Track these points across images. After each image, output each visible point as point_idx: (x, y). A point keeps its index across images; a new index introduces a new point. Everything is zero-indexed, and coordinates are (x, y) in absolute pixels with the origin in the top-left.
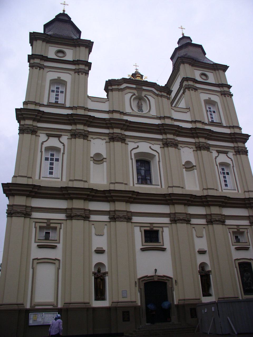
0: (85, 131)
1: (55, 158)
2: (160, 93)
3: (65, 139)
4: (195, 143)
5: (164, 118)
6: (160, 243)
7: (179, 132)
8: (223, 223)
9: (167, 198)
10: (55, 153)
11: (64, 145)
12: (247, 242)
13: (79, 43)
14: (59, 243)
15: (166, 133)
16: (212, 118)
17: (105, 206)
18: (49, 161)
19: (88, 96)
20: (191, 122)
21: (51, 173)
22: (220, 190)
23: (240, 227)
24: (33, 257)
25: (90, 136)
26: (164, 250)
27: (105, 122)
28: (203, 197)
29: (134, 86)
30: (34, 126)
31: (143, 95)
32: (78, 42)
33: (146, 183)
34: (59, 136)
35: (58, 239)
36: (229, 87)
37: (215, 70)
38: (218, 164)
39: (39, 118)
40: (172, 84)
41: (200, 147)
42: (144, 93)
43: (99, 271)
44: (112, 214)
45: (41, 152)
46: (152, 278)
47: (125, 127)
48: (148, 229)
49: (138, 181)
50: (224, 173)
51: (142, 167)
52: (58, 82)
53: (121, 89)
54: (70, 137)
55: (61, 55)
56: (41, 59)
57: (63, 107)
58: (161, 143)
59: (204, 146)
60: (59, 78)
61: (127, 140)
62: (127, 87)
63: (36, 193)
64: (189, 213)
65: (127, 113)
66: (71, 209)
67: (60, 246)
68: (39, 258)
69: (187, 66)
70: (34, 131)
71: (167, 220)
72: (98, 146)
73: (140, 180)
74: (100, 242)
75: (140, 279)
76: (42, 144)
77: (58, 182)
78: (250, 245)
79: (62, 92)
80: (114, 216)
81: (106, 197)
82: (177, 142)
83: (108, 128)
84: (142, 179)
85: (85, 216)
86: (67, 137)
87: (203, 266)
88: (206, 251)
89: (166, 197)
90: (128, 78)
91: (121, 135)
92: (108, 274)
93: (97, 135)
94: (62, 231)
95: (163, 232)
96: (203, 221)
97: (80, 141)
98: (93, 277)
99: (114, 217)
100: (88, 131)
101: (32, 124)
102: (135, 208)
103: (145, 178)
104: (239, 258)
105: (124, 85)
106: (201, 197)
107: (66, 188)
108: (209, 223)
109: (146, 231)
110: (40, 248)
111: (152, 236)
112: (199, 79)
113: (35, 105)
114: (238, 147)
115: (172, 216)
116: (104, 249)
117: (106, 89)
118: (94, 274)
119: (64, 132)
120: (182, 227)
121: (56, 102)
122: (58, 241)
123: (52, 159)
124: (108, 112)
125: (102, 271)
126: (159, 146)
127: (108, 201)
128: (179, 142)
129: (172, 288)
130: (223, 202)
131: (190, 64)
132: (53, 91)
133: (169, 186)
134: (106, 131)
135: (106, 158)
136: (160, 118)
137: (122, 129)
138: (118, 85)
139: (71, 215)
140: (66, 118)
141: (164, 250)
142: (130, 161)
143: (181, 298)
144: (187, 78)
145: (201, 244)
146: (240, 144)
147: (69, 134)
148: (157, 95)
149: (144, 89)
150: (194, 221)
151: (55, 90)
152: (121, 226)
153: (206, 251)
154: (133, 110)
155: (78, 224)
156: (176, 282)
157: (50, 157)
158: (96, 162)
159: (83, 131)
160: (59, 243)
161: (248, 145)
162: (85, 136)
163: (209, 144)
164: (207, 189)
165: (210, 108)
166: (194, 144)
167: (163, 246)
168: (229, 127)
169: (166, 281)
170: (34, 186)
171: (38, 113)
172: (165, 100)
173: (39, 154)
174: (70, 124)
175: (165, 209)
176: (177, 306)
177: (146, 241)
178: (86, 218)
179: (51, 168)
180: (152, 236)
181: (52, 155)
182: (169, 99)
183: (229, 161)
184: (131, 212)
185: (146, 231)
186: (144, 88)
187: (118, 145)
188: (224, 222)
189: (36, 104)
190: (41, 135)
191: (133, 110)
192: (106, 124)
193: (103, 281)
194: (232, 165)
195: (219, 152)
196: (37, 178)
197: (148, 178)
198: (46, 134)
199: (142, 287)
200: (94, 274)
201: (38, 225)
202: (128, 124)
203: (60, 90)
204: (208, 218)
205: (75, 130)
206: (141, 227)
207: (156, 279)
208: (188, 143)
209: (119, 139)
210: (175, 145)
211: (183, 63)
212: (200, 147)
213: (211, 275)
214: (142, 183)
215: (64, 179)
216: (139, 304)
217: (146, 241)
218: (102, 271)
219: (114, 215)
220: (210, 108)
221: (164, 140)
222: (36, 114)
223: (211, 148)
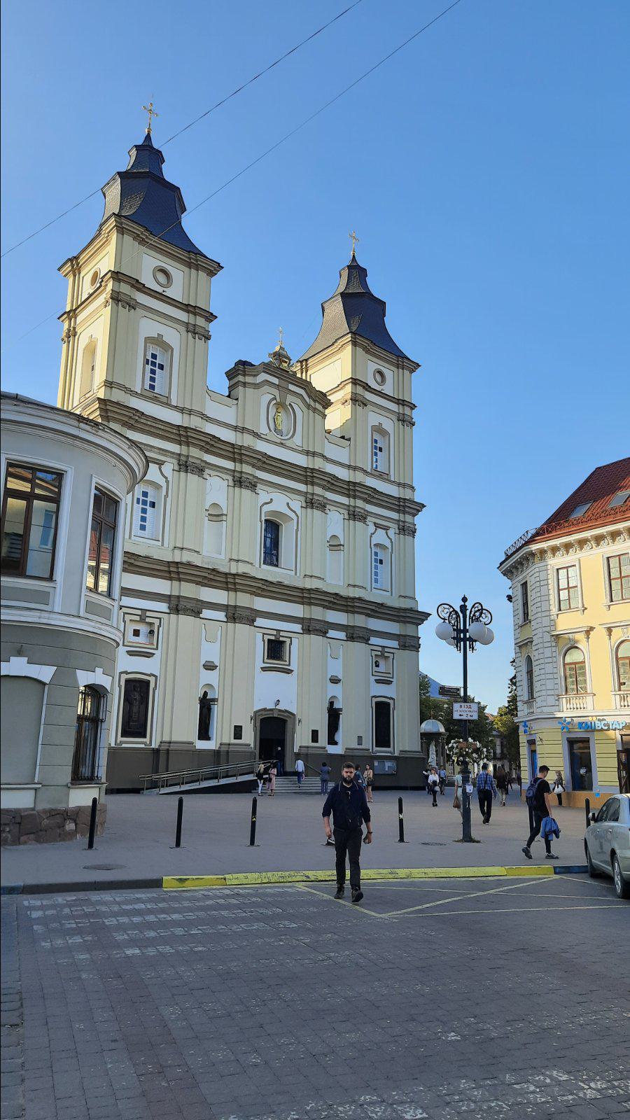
0: (202, 461)
1: (149, 499)
2: (312, 403)
3: (169, 468)
4: (349, 506)
5: (314, 454)
6: (286, 661)
7: (333, 484)
8: (366, 641)
10: (150, 490)
11: (167, 482)
12: (390, 673)
14: (157, 649)
15: (313, 484)
17: (220, 596)
19: (208, 391)
20: (349, 467)
21: (143, 528)
22: (369, 588)
23: (386, 650)
24: (119, 668)
26: (289, 672)
27: (231, 449)
28: (349, 600)
29: (276, 381)
31: (287, 403)
32: (197, 260)
33: (272, 564)
35: (155, 643)
36: (413, 407)
38: (372, 546)
39: (132, 422)
41: (354, 516)
42: (290, 399)
46: (271, 712)
48: (273, 638)
53: (258, 384)
54: (177, 468)
56: (133, 286)
58: (303, 499)
62: (266, 381)
65: (262, 436)
71: (297, 628)
72: (216, 489)
74: (211, 652)
75: (256, 713)
78: (393, 678)
80: (234, 614)
81: (227, 583)
82: (325, 501)
83: (234, 460)
85: (195, 609)
90: (267, 360)
92: (217, 701)
95: (291, 644)
99: (235, 615)
100: (205, 462)
102: (261, 604)
103: (272, 554)
104: (377, 695)
105: (263, 377)
106: (347, 599)
108: (349, 639)
110: (130, 655)
114: (404, 522)
117: (231, 375)
120: (315, 639)
121: (152, 387)
122: (155, 647)
123: (145, 503)
127: (228, 589)
130: (372, 610)
134: (229, 465)
136: (308, 453)
137: (253, 466)
139: (178, 606)
140: (174, 431)
145: (336, 668)
146: (408, 518)
148: (308, 406)
149: (290, 390)
150: (332, 633)
151: (150, 359)
152: (241, 628)
155: (186, 621)
156: (299, 721)
157: (141, 498)
158: (211, 518)
159: (198, 462)
160: (157, 649)
161: (420, 520)
162: (200, 470)
163: (368, 511)
164: (354, 586)
167: (289, 665)
168: (399, 484)
177: (269, 657)
178: (196, 613)
180: (275, 649)
183: (387, 543)
186: (291, 387)
187: (246, 493)
188: (369, 639)
192: (234, 453)
193: (209, 710)
194: (390, 551)
199: (258, 724)
201: (128, 617)
202: (265, 460)
203: (158, 362)
205: (188, 456)
208: (338, 505)
217: (269, 657)
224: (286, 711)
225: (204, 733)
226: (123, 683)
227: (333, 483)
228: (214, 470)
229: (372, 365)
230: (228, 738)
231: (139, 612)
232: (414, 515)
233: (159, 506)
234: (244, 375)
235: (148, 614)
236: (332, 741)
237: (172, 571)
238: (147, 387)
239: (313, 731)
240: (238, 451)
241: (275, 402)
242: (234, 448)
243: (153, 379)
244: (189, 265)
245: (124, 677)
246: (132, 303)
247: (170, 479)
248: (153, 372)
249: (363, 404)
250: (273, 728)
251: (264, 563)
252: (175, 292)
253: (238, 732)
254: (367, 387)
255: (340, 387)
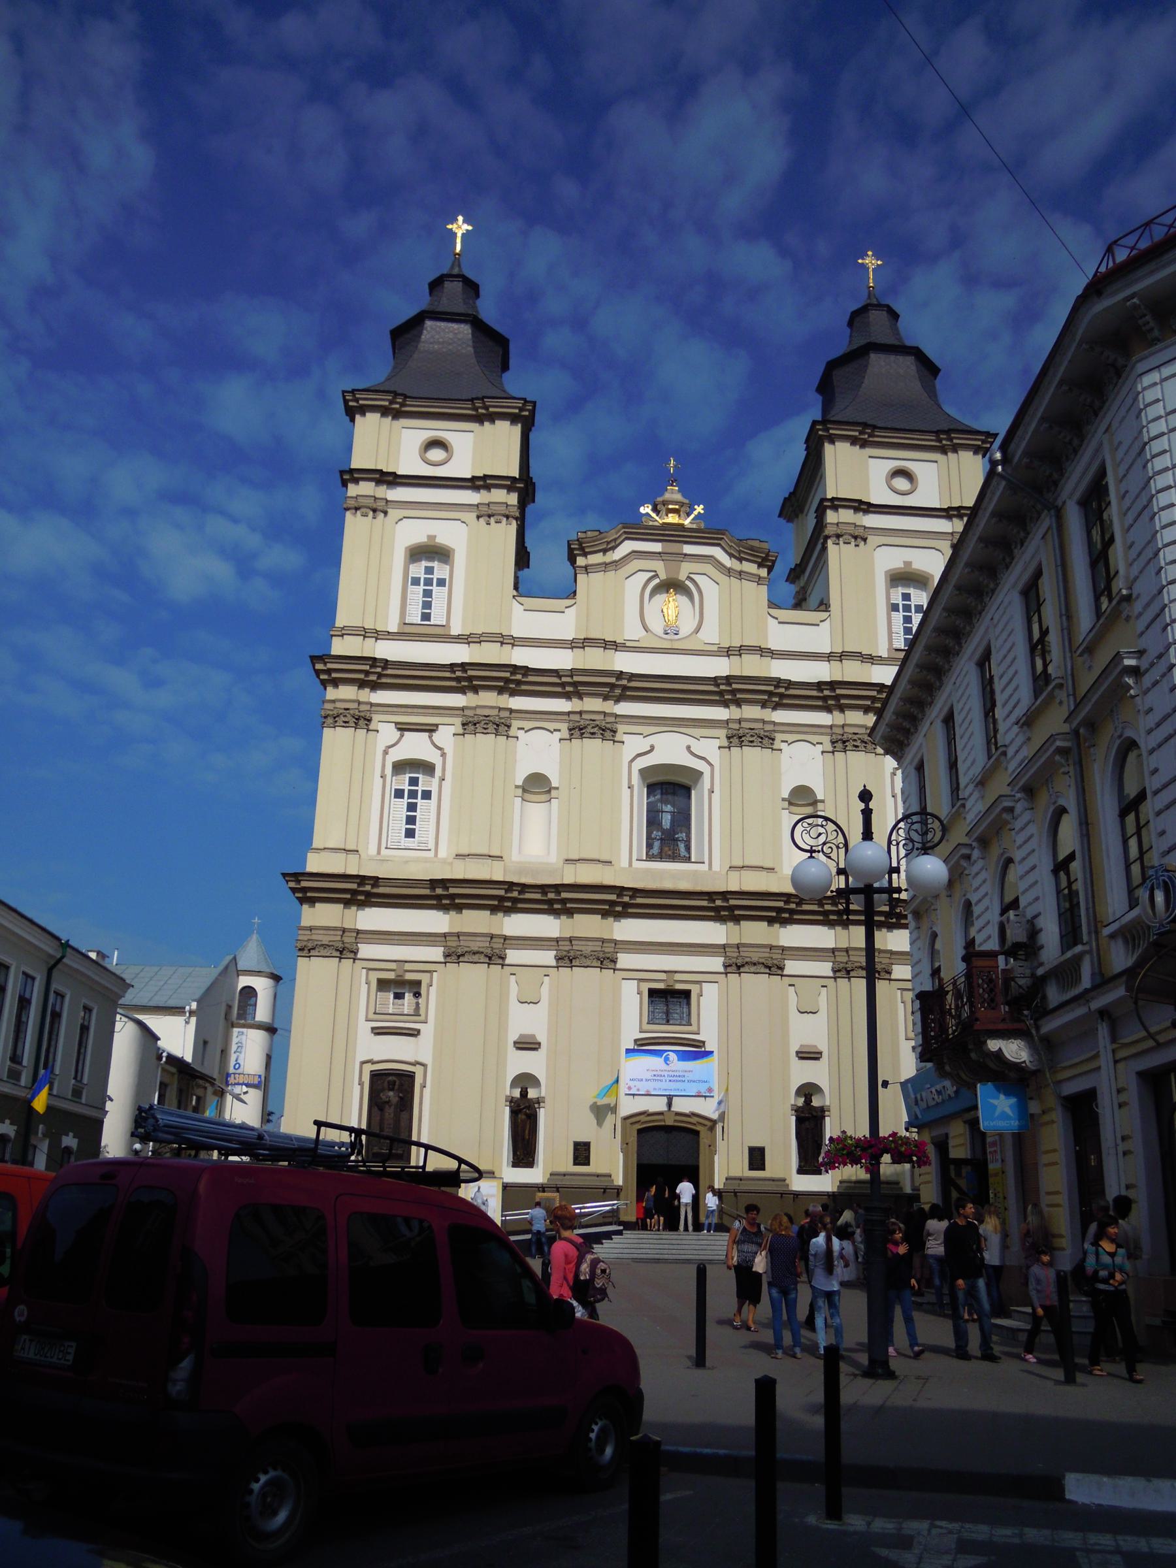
0: (500, 709)
1: (420, 788)
3: (446, 735)
4: (831, 727)
5: (741, 651)
9: (719, 903)
11: (443, 755)
13: (491, 410)
15: (738, 703)
18: (405, 800)
20: (829, 657)
21: (410, 834)
29: (657, 547)
30: (360, 703)
31: (682, 576)
32: (487, 408)
33: (674, 857)
34: (431, 729)
37: (943, 450)
39: (373, 678)
40: (810, 492)
41: (844, 742)
42: (685, 570)
43: (524, 1093)
44: (565, 946)
46: (660, 1117)
47: (618, 691)
48: (661, 986)
49: (649, 846)
51: (666, 804)
52: (430, 552)
55: (436, 454)
56: (379, 482)
58: (722, 733)
59: (855, 737)
60: (432, 538)
63: (368, 894)
64: (781, 944)
65: (628, 644)
66: (458, 935)
67: (427, 1030)
68: (376, 1059)
69: (843, 447)
70: (361, 719)
71: (716, 963)
72: (539, 749)
73: (657, 844)
74: (525, 1020)
75: (625, 1119)
76: (386, 752)
77: (426, 860)
79: (441, 582)
80: (568, 951)
82: (769, 727)
83: (567, 696)
84: (661, 839)
85: (493, 953)
86: (452, 729)
87: (808, 1091)
88: (821, 1053)
89: (714, 901)
91: (602, 717)
93: (536, 720)
94: (433, 990)
96: (825, 968)
97: (485, 742)
98: (507, 1109)
99: (569, 955)
100: (511, 711)
101: (353, 697)
105: (627, 547)
107: (444, 883)
109: (652, 993)
112: (879, 494)
113: (365, 637)
115: (733, 953)
116: (539, 1039)
118: (511, 1101)
120: (756, 983)
121: (426, 617)
124: (572, 641)
125: (532, 1094)
126: (717, 743)
128: (777, 728)
129: (712, 1147)
131: (854, 441)
132: (416, 581)
133: (735, 863)
135: (557, 788)
136: (728, 652)
137: (606, 698)
138: (605, 551)
139: (457, 951)
140: (448, 675)
142: (626, 792)
143: (733, 1174)
144: (833, 499)
148: (729, 572)
150: (792, 967)
152: (586, 978)
153: (821, 1053)
154: (646, 629)
155: (473, 974)
157: (406, 788)
159: (495, 712)
162: (499, 725)
165: (906, 597)
166: (829, 731)
169: (698, 1128)
170: (362, 879)
171: (371, 666)
172: (749, 586)
173: (378, 781)
174: (462, 690)
175: (713, 932)
179: (411, 820)
181: (414, 782)
182: (759, 580)
184: (616, 942)
185: (652, 993)
186: (688, 549)
187: (593, 746)
189: (365, 633)
190: (381, 727)
191: (646, 629)
192: (563, 685)
193: (533, 1118)
196: (372, 850)
198: (396, 723)
199: (633, 1139)
200: (511, 1101)
202: (624, 682)
203: (435, 577)
204: (838, 959)
206: (640, 980)
207: (670, 1122)
208: (805, 729)
209: (595, 730)
210: (764, 738)
211: (832, 442)
212: (844, 742)
213: (827, 1119)
214: (661, 857)
215: (443, 853)
216: (619, 1181)
218: (532, 1094)
219: (567, 948)
220: (906, 597)
221: (731, 725)
222: (367, 668)
224: (694, 1115)
225: (524, 1153)
226: (366, 1079)
227: (780, 694)
228: (530, 719)
230: (566, 1164)
231: (393, 966)
233: (434, 795)
234: (585, 555)
235: (407, 966)
237: (442, 894)
238: (417, 620)
239: (752, 1150)
240: (568, 679)
241: (657, 581)
242: (560, 677)
243: (427, 605)
244: (479, 419)
245: (368, 1068)
246: (380, 505)
247: (449, 751)
248: (428, 593)
249: (856, 538)
251: (650, 857)
252: (460, 467)
253: (582, 1152)
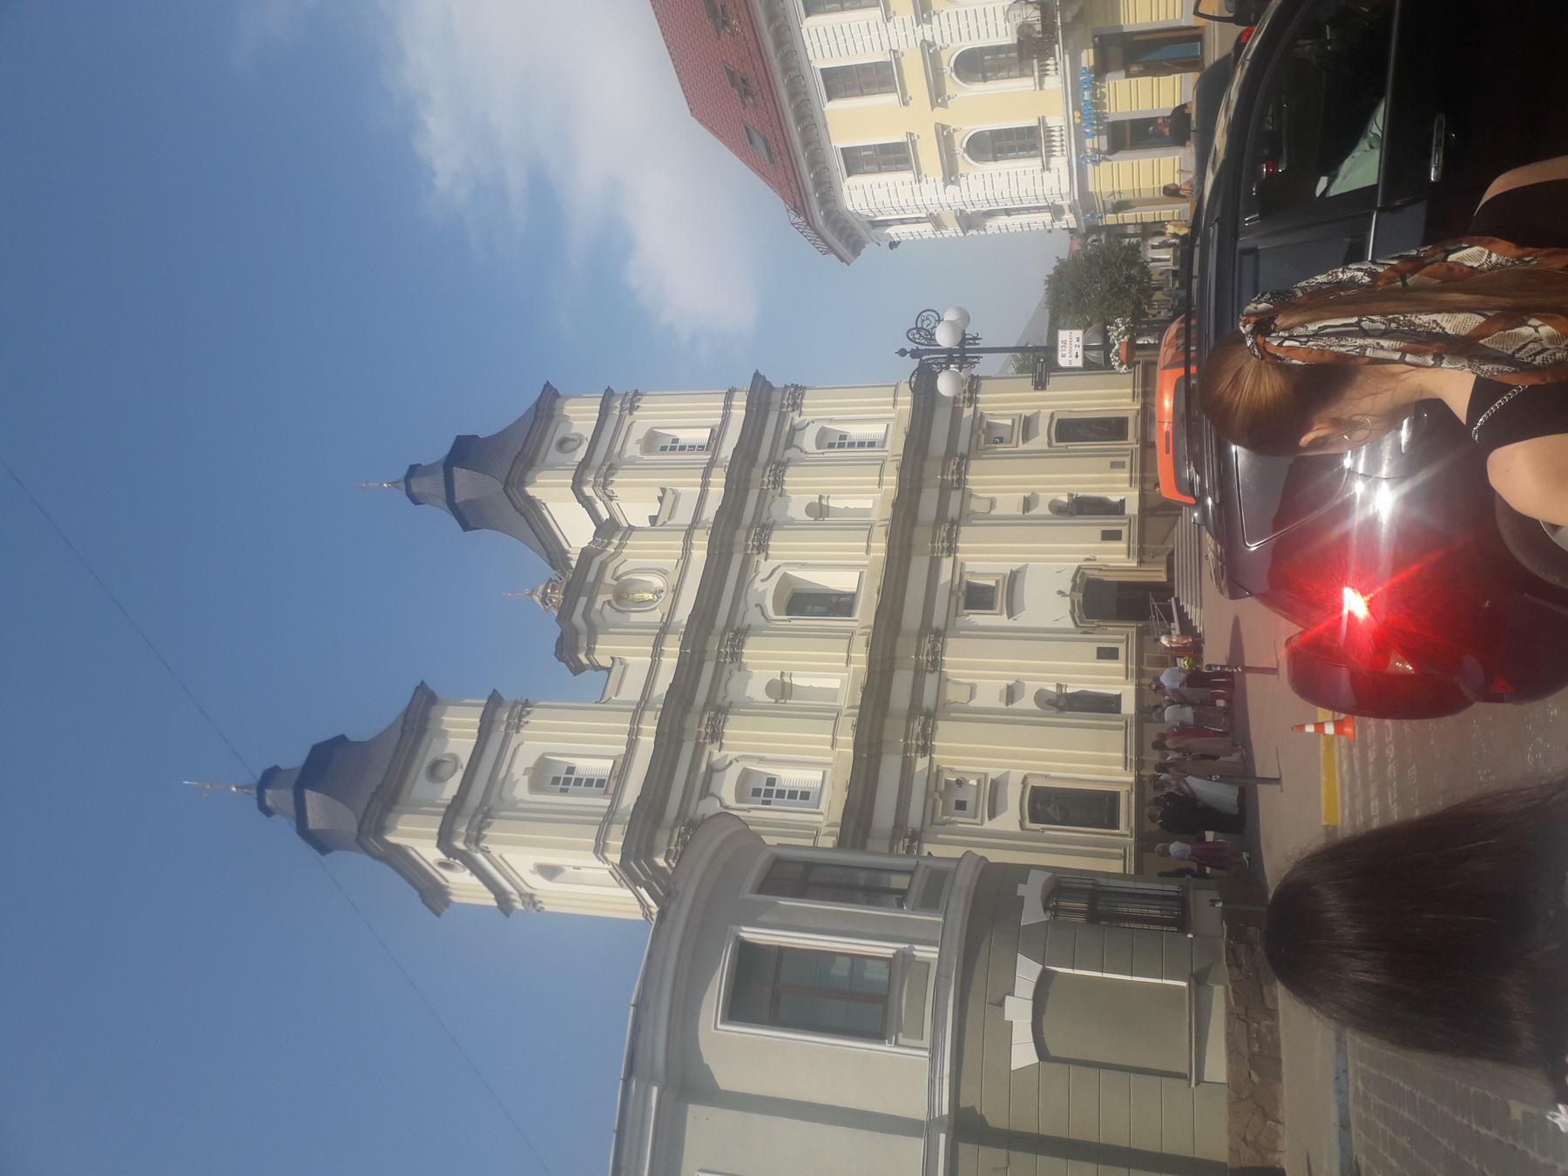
1: (764, 787)
16: (692, 447)
21: (805, 795)
25: (719, 701)
26: (1014, 578)
29: (583, 601)
34: (711, 770)
37: (550, 417)
45: (749, 810)
48: (962, 602)
50: (841, 445)
57: (623, 766)
61: (737, 623)
100: (706, 704)
105: (577, 619)
111: (978, 597)
117: (578, 669)
119: (701, 756)
121: (601, 783)
138: (577, 632)
141: (1014, 578)
146: (776, 397)
147: (709, 748)
157: (762, 798)
160: (986, 775)
165: (664, 449)
173: (753, 813)
176: (1141, 562)
186: (591, 578)
190: (700, 812)
193: (1075, 696)
195: (790, 444)
196: (820, 818)
197: (834, 600)
199: (1096, 622)
207: (1079, 596)
211: (522, 483)
220: (664, 449)
223: (778, 457)
224: (1074, 580)
229: (553, 455)
231: (930, 801)
232: (771, 388)
235: (932, 788)
236: (1118, 509)
243: (589, 782)
250: (1102, 601)
254: (585, 465)
255: (587, 503)
